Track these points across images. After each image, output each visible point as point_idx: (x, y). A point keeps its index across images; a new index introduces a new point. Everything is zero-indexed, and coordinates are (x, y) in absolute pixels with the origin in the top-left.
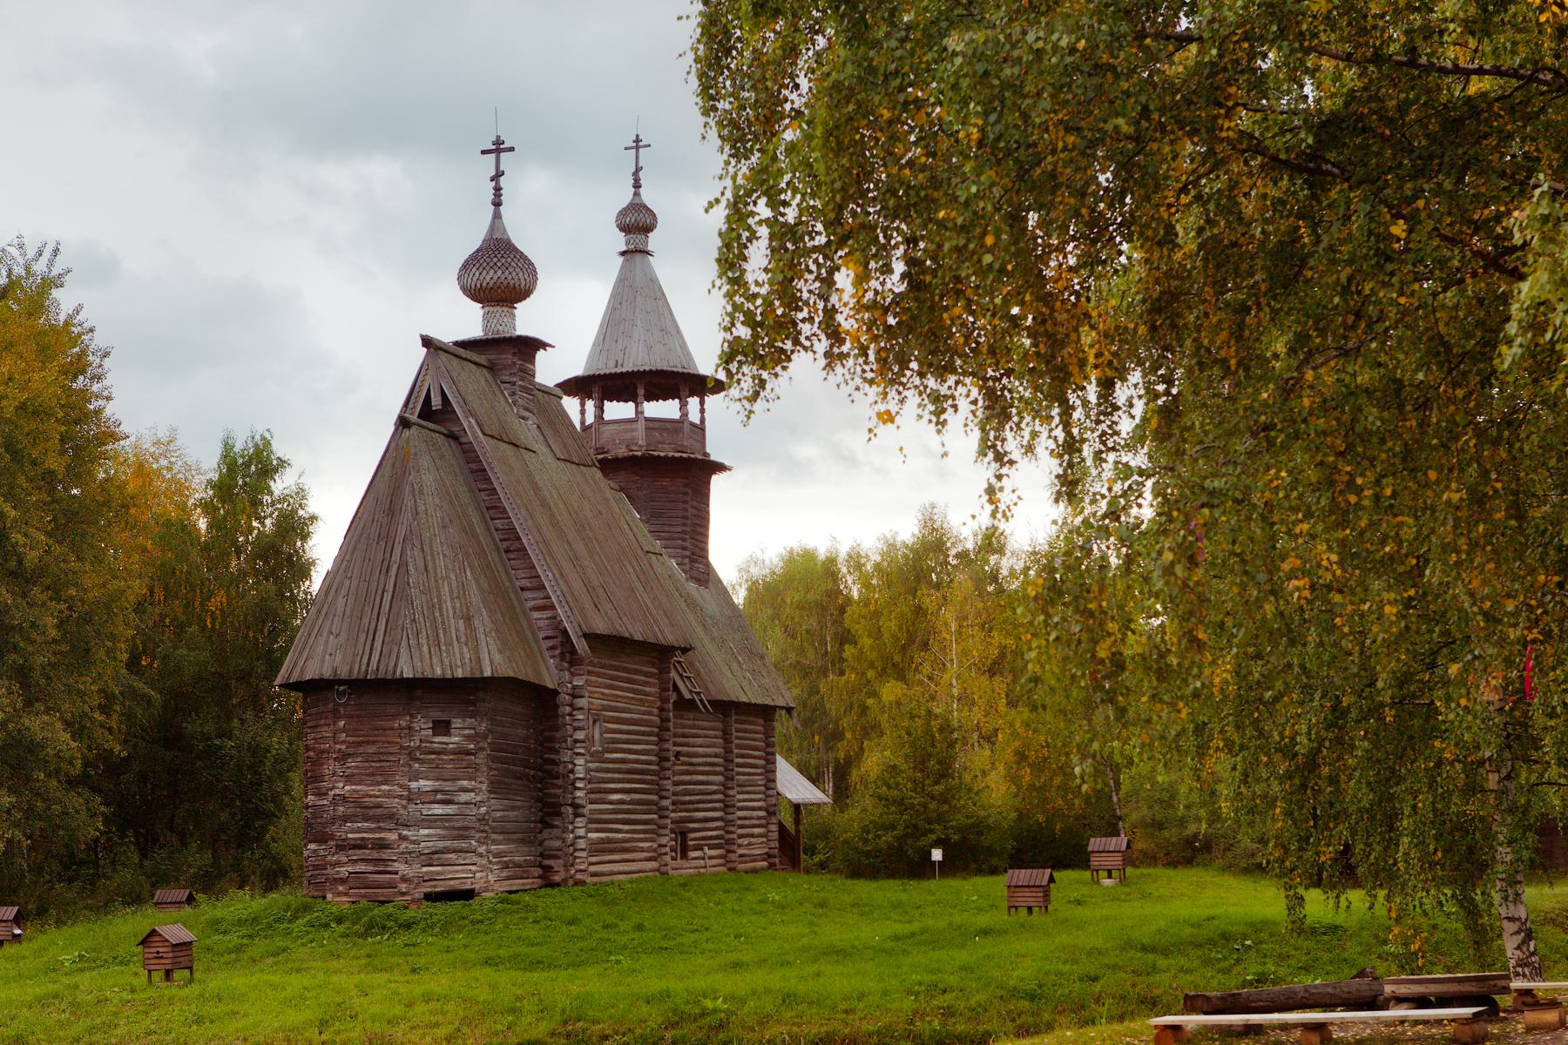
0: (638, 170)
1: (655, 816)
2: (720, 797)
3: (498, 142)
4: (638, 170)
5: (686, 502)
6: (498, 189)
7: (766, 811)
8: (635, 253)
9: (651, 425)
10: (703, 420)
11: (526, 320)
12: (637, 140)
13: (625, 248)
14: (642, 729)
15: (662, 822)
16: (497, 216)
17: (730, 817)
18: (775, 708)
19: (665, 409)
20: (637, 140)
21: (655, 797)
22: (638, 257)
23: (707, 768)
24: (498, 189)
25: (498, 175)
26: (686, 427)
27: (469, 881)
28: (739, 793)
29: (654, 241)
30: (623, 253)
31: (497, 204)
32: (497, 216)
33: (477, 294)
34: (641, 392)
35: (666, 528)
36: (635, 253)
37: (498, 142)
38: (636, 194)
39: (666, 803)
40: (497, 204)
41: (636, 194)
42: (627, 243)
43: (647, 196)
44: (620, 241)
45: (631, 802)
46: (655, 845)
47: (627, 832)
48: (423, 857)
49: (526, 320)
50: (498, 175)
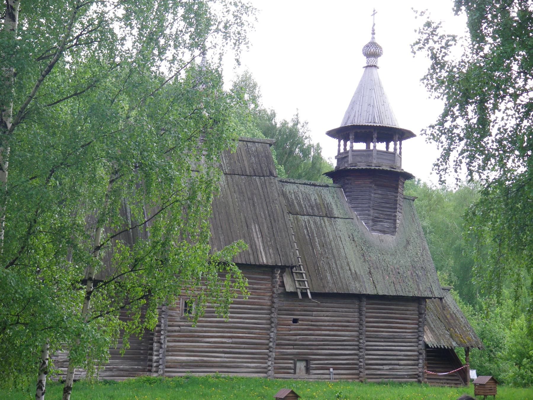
0: (374, 25)
1: (268, 351)
2: (357, 343)
4: (374, 25)
5: (370, 192)
7: (418, 352)
9: (355, 153)
13: (366, 65)
14: (249, 306)
15: (270, 354)
17: (361, 354)
18: (425, 298)
19: (381, 146)
21: (267, 342)
22: (374, 69)
23: (340, 328)
26: (396, 155)
27: (78, 376)
28: (367, 341)
30: (366, 67)
34: (375, 135)
35: (360, 205)
38: (373, 38)
39: (271, 344)
41: (373, 38)
42: (367, 63)
44: (364, 61)
45: (232, 343)
46: (265, 365)
47: (227, 358)
48: (59, 363)
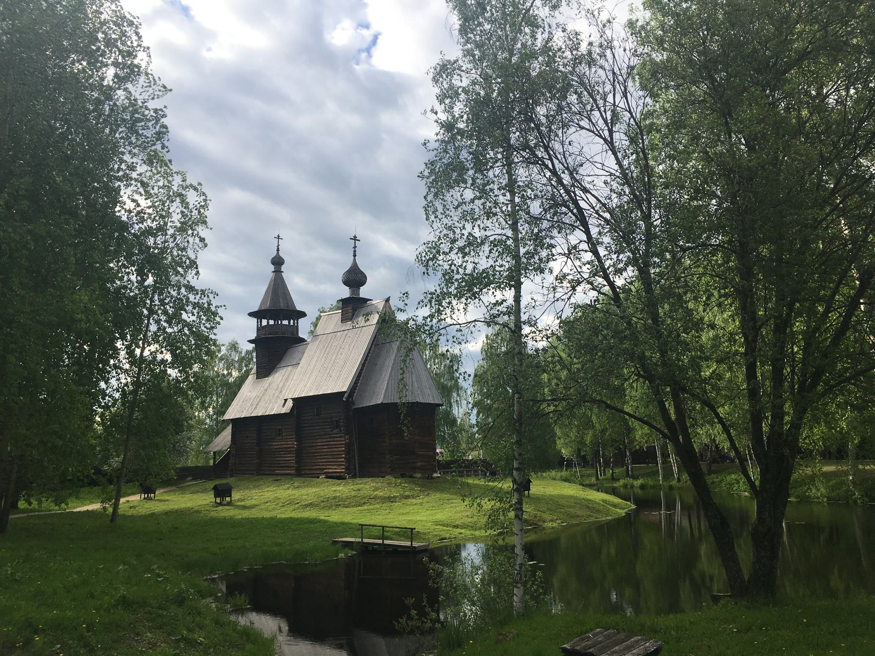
0: (278, 245)
3: (355, 237)
4: (278, 245)
6: (355, 251)
8: (278, 272)
10: (298, 325)
11: (364, 292)
12: (279, 236)
16: (355, 260)
20: (279, 236)
24: (355, 251)
25: (355, 247)
29: (283, 268)
30: (273, 272)
31: (355, 256)
32: (355, 260)
33: (346, 283)
36: (278, 272)
37: (355, 237)
38: (278, 253)
40: (355, 256)
41: (278, 253)
43: (281, 254)
44: (272, 268)
49: (364, 292)
50: (355, 247)
